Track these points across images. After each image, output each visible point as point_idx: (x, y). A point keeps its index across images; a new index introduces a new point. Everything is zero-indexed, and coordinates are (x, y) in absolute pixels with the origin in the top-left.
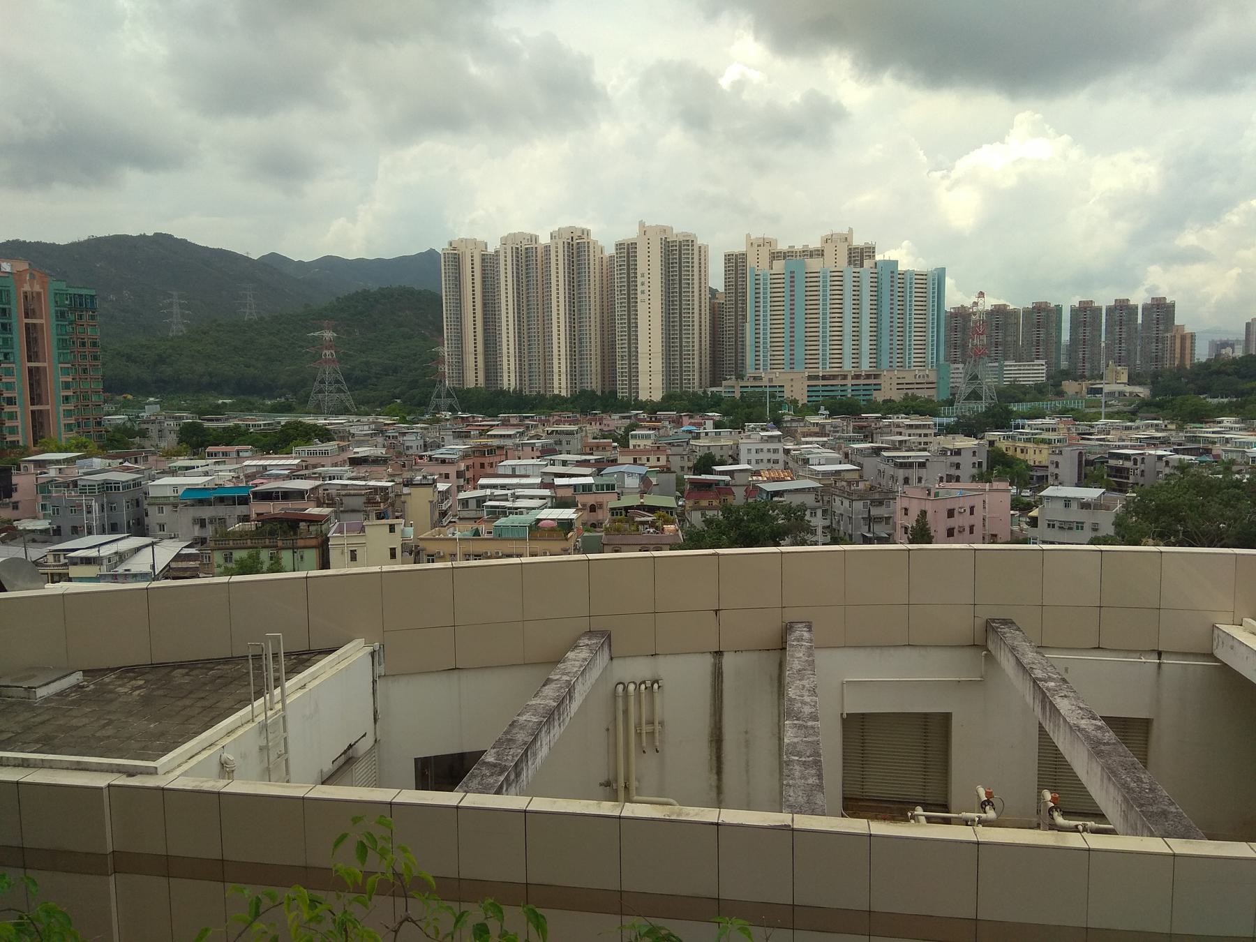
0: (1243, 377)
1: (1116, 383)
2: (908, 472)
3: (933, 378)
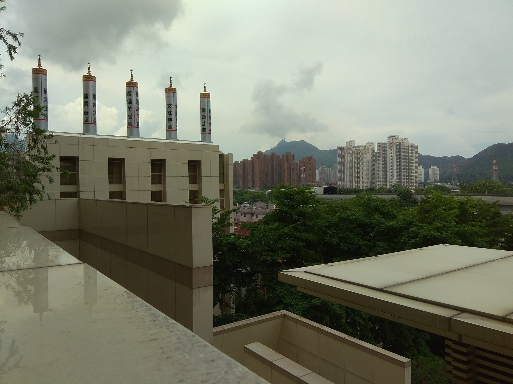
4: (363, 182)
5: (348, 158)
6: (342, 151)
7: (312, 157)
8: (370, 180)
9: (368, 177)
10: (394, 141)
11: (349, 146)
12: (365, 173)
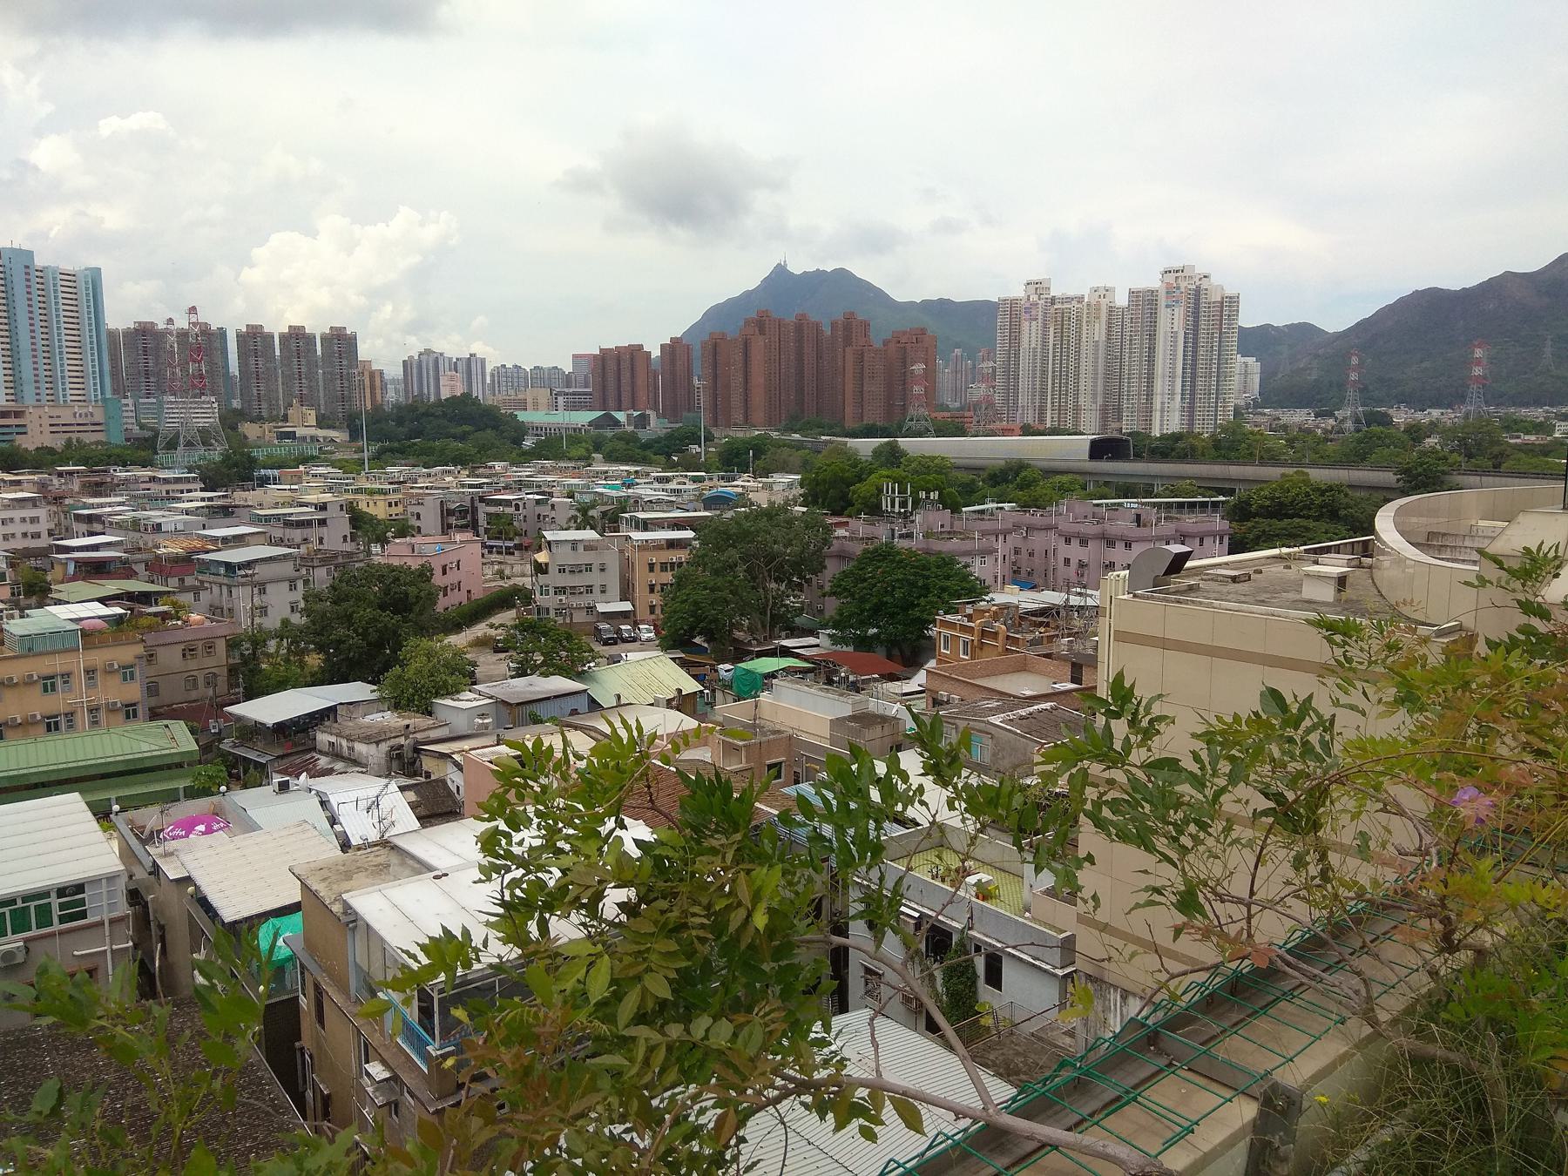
1: (305, 424)
2: (307, 532)
3: (99, 417)
4: (1077, 409)
5: (1030, 334)
6: (1012, 309)
7: (923, 332)
8: (1100, 400)
9: (1095, 395)
10: (1183, 285)
11: (1034, 298)
12: (1085, 384)
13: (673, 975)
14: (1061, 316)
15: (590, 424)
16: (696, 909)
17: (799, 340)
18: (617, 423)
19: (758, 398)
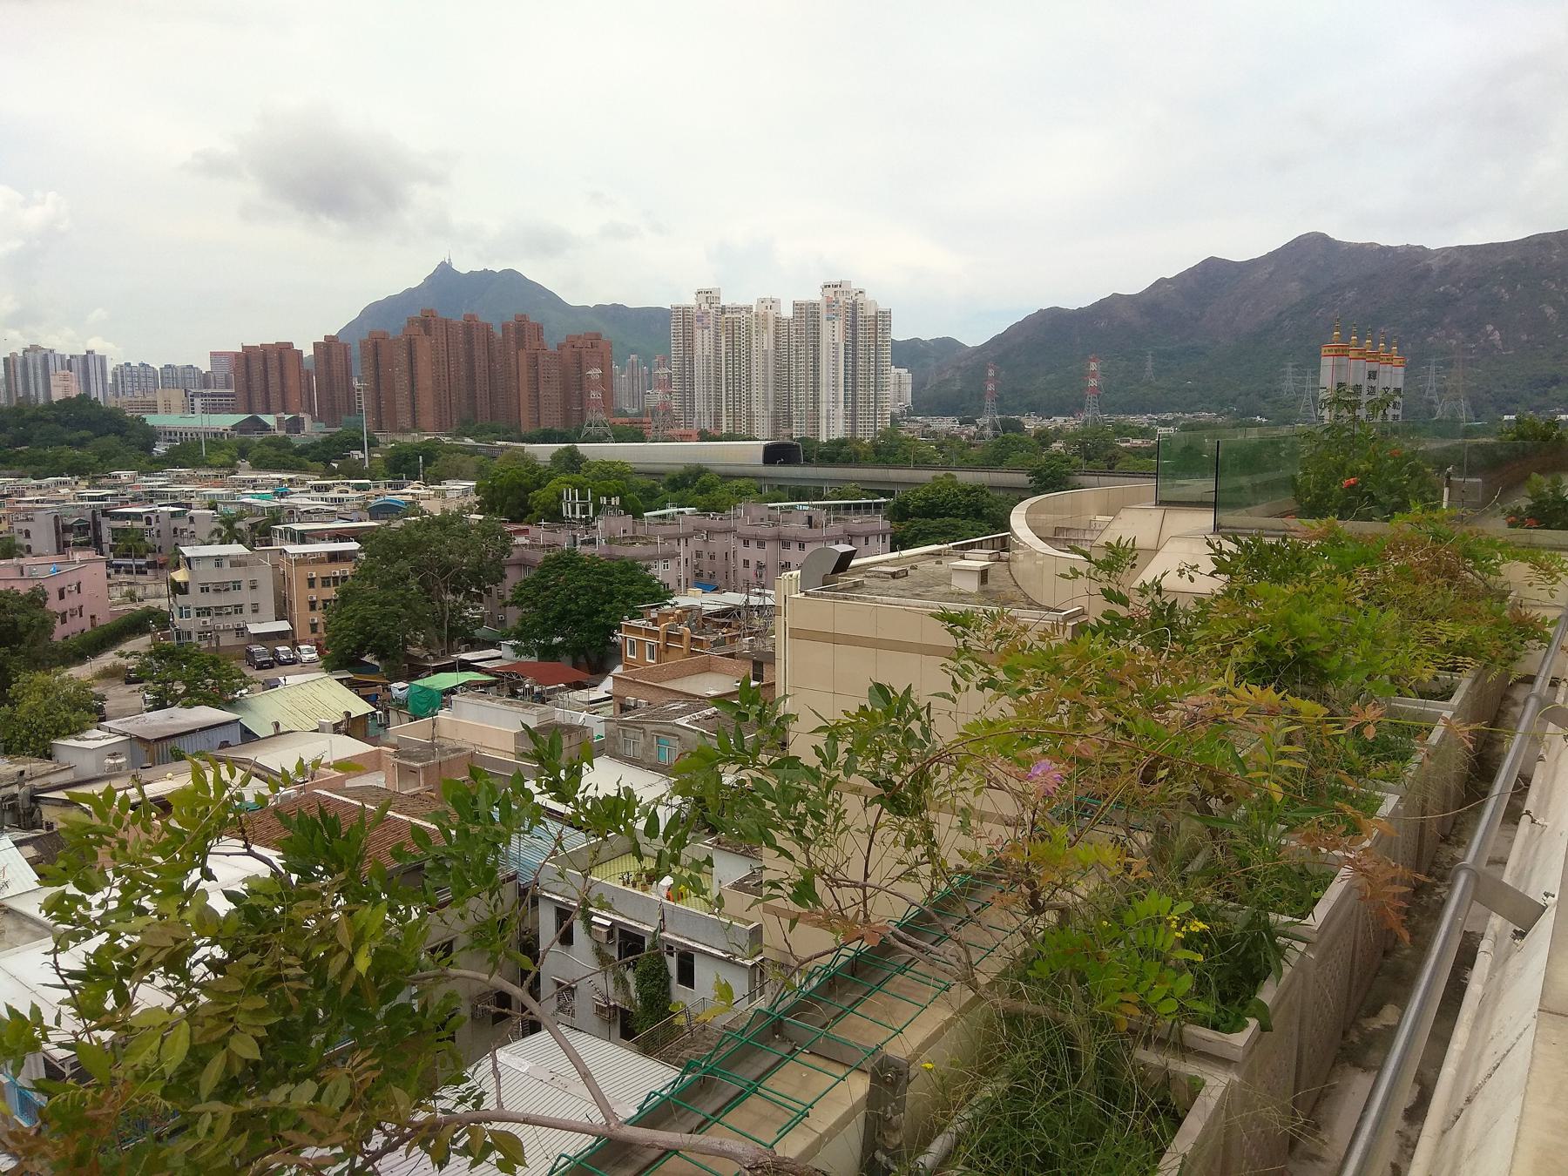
0: (65, 424)
4: (750, 415)
5: (703, 342)
6: (685, 318)
7: (598, 336)
8: (771, 407)
9: (766, 402)
10: (842, 299)
11: (705, 306)
13: (262, 1033)
14: (732, 326)
15: (234, 428)
16: (291, 960)
17: (469, 342)
18: (266, 427)
19: (426, 401)
